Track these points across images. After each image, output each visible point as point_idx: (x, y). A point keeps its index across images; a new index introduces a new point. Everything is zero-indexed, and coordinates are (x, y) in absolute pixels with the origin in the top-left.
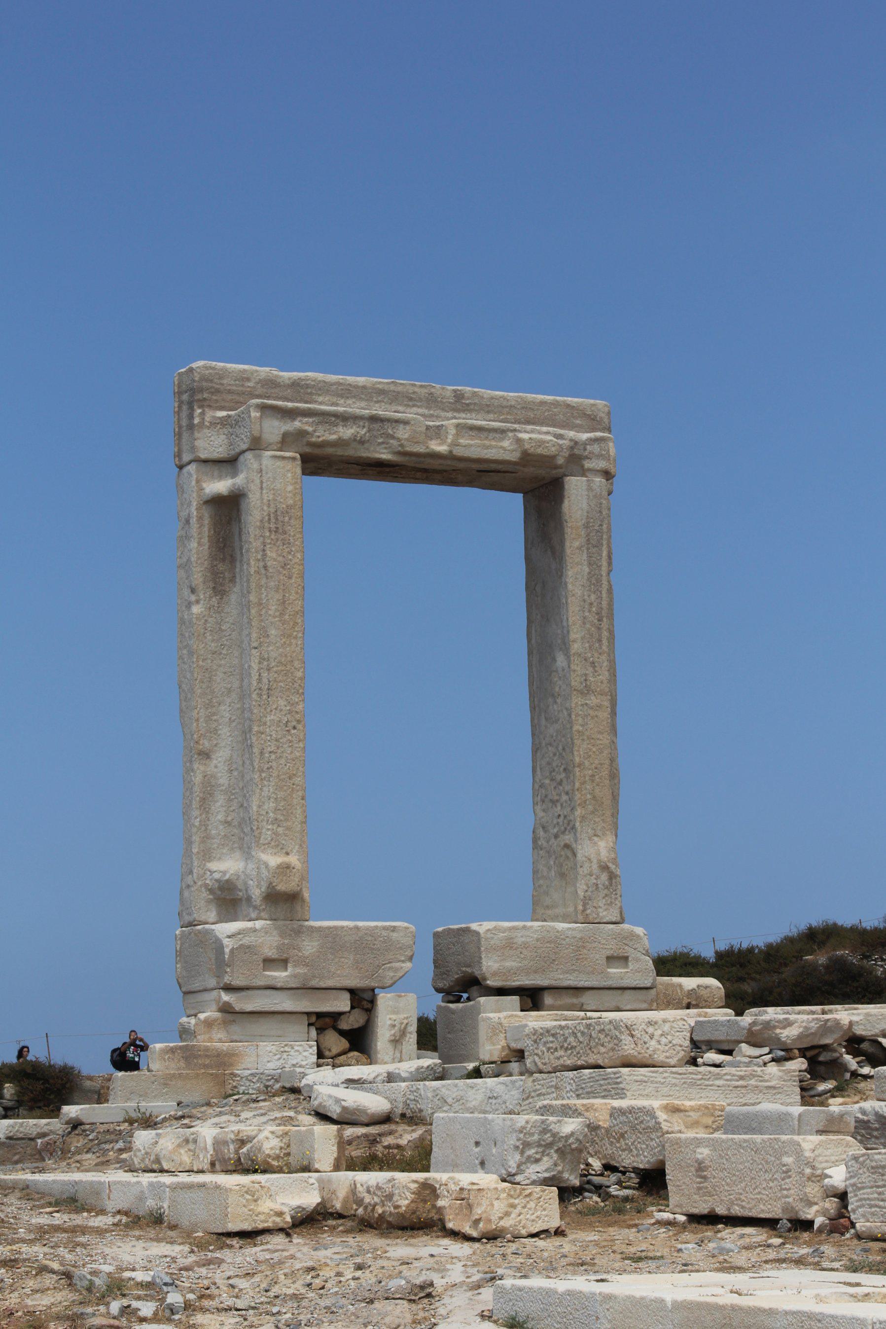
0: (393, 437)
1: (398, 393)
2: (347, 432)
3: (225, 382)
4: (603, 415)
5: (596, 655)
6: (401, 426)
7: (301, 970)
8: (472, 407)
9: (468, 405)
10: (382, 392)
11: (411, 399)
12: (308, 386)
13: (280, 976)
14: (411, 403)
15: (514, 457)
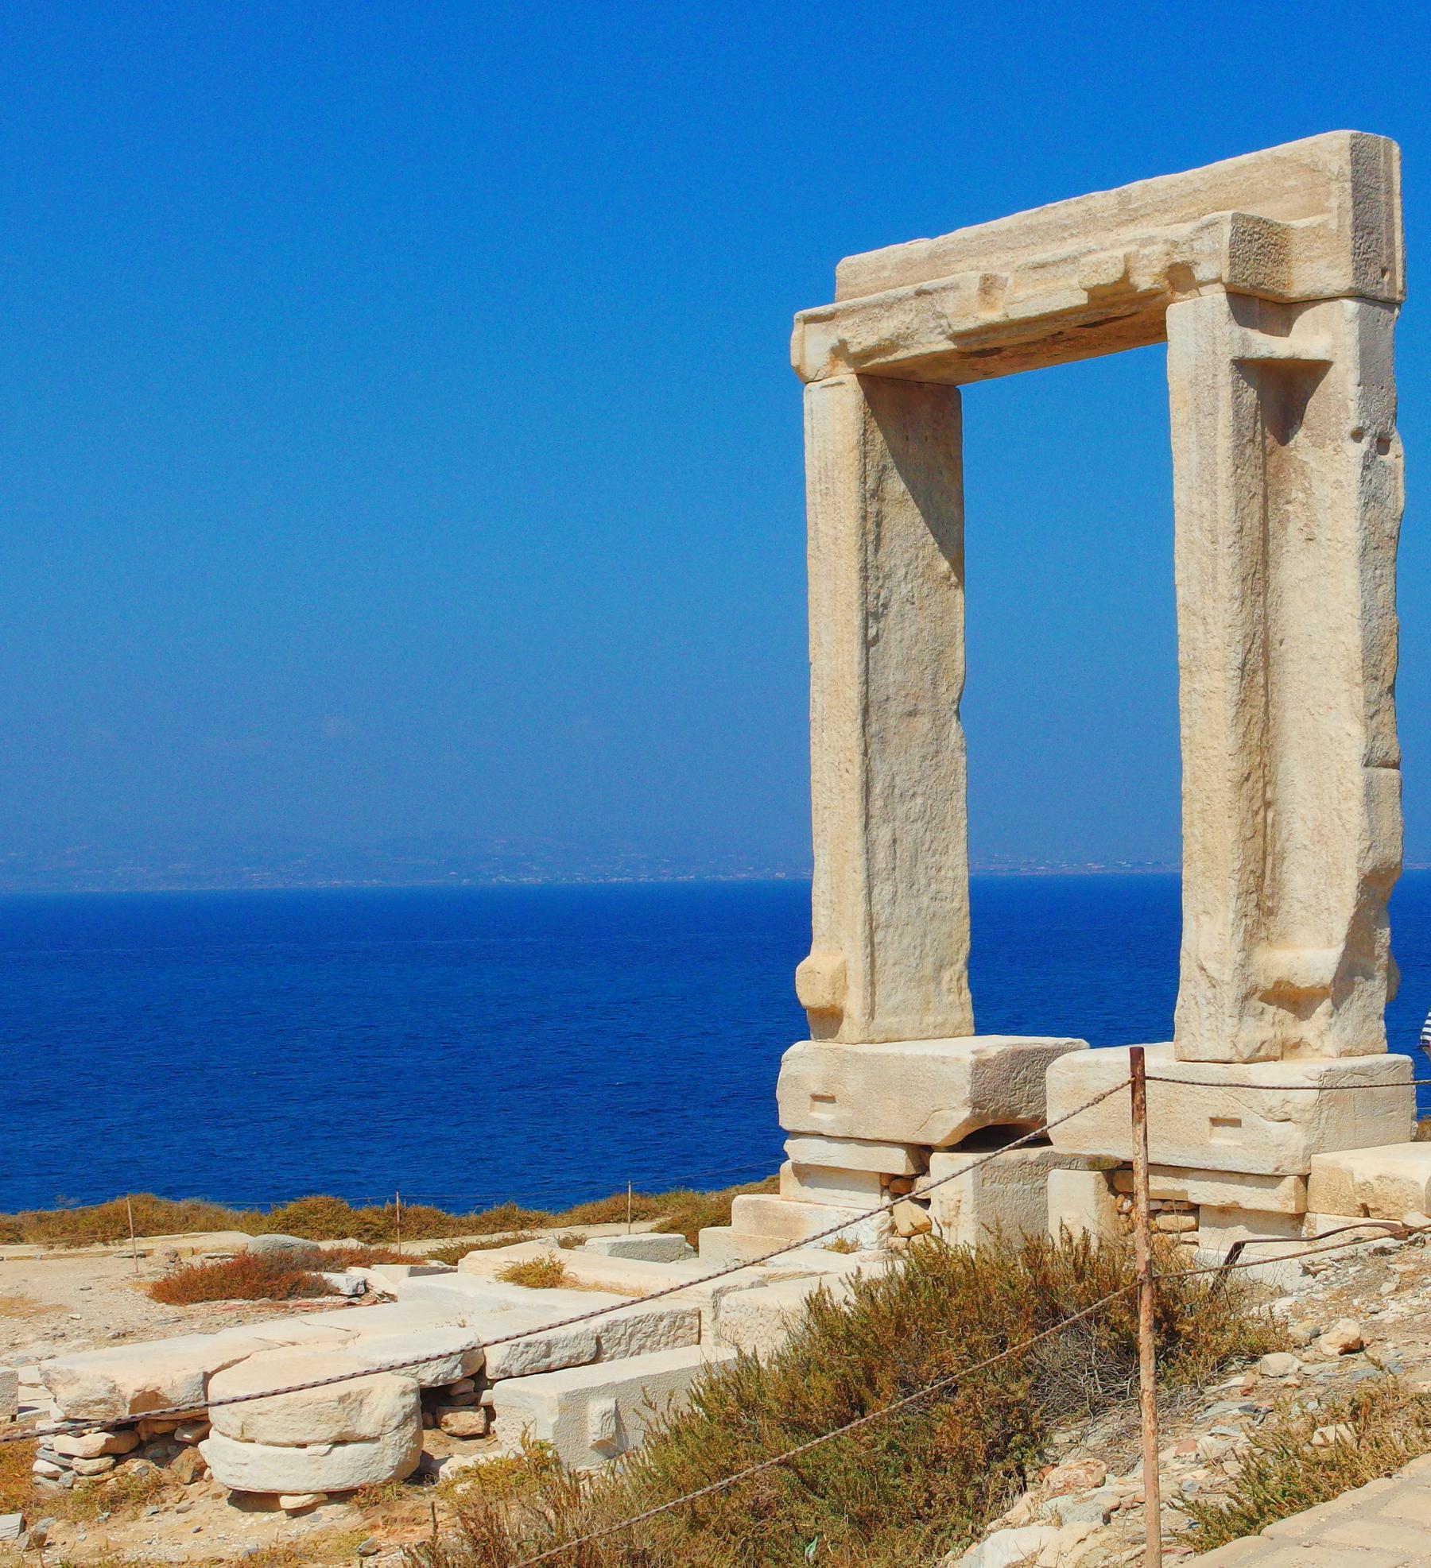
0: (944, 316)
1: (1050, 223)
2: (888, 327)
3: (860, 280)
4: (1328, 157)
5: (1210, 603)
6: (951, 294)
7: (846, 1113)
8: (1142, 212)
9: (1135, 210)
10: (1031, 229)
11: (1065, 227)
12: (946, 253)
13: (824, 1117)
14: (1066, 234)
15: (1081, 299)
